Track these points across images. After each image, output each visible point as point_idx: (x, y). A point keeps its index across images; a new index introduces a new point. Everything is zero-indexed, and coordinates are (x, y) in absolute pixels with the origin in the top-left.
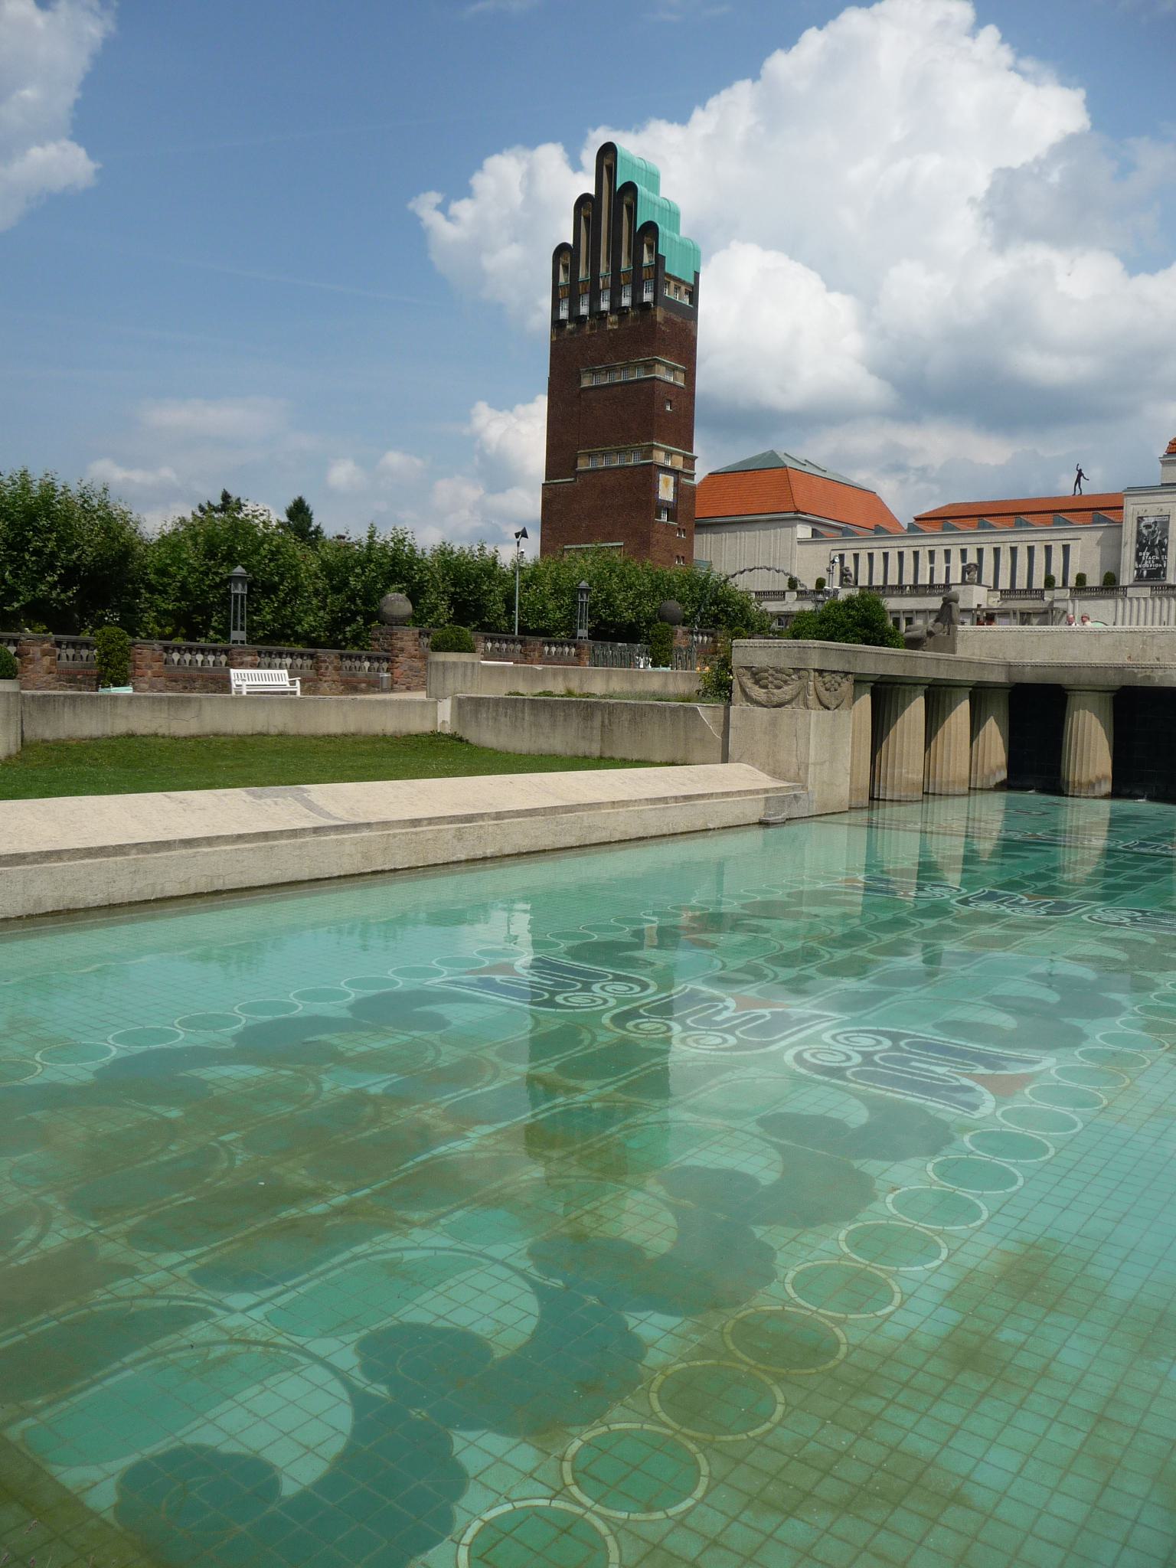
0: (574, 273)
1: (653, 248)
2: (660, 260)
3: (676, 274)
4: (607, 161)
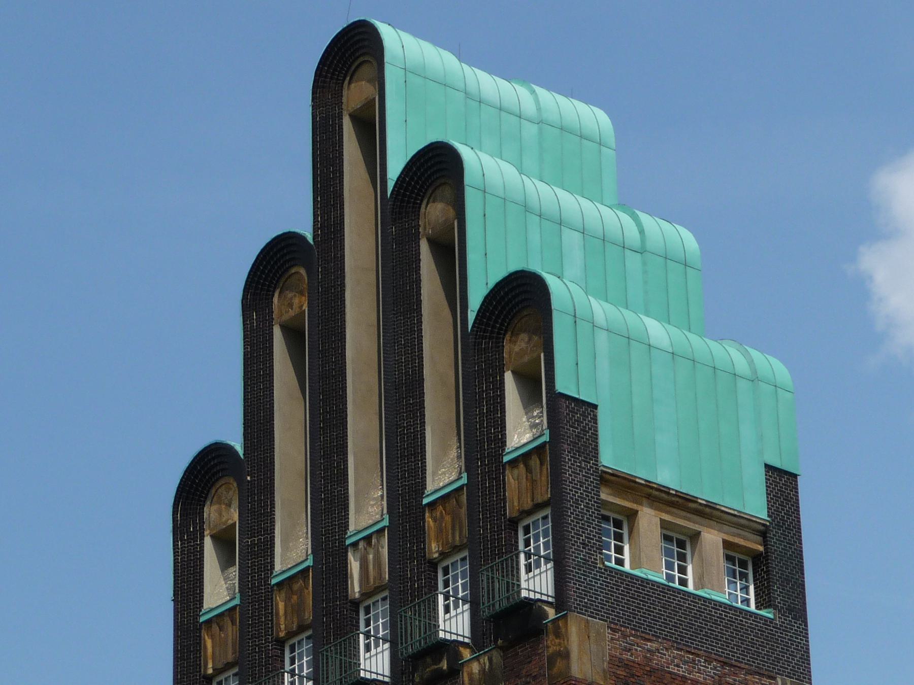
0: (251, 548)
1: (536, 383)
2: (572, 422)
3: (666, 476)
4: (355, 94)
